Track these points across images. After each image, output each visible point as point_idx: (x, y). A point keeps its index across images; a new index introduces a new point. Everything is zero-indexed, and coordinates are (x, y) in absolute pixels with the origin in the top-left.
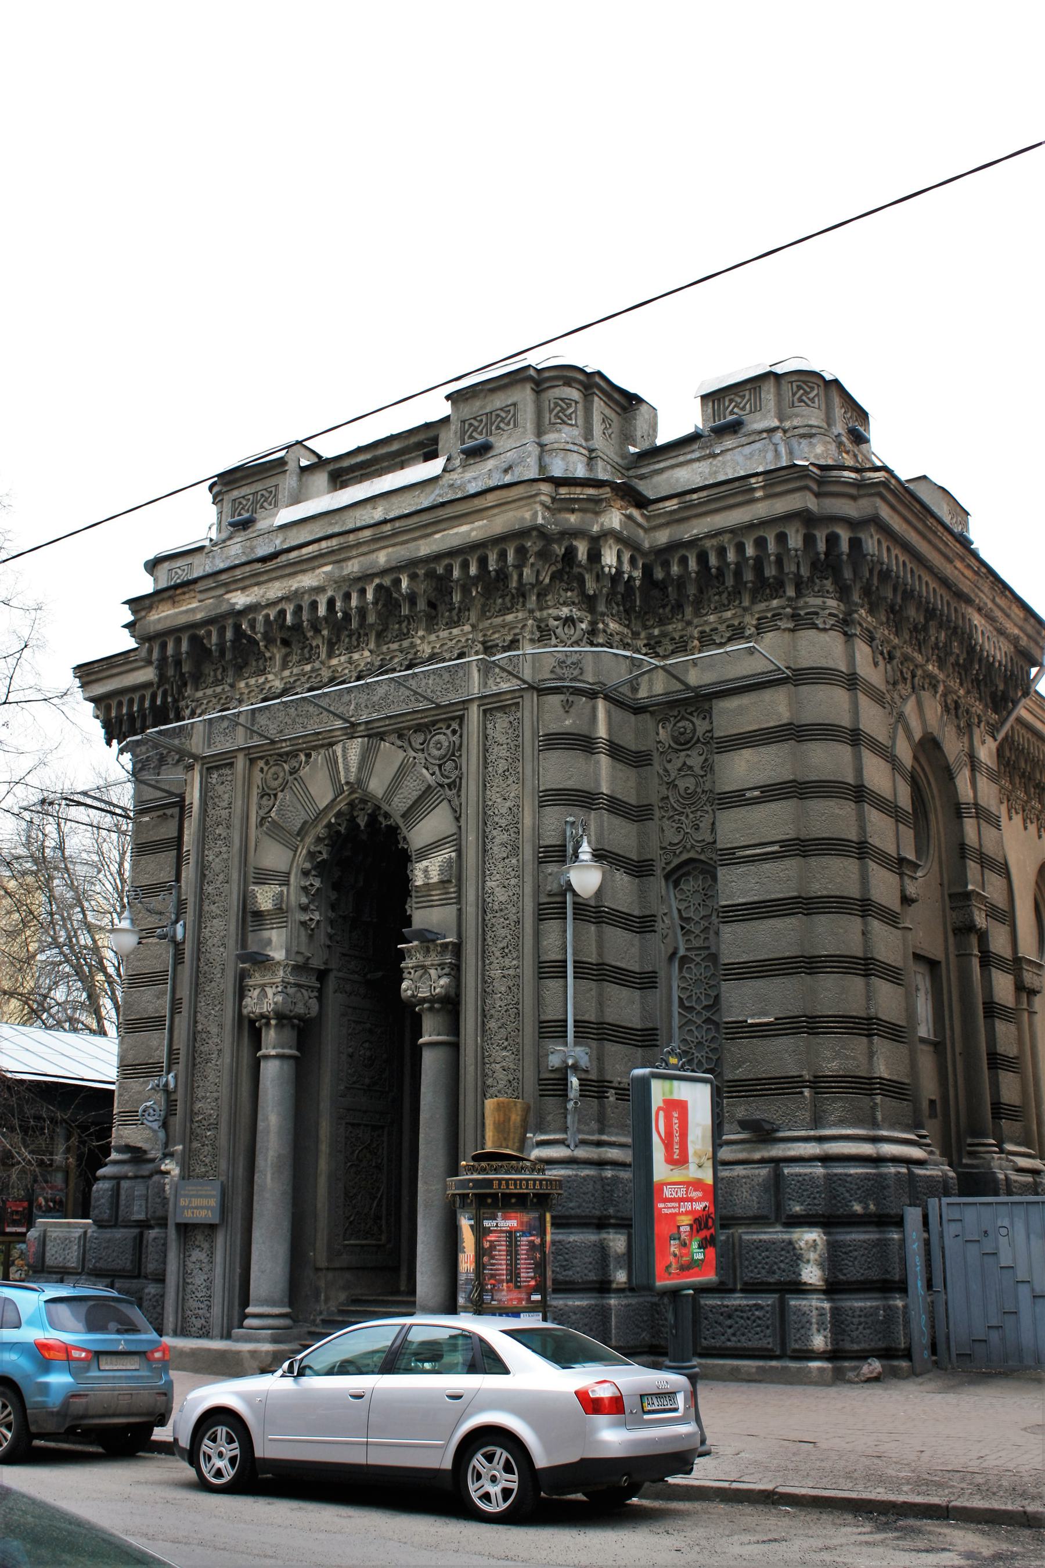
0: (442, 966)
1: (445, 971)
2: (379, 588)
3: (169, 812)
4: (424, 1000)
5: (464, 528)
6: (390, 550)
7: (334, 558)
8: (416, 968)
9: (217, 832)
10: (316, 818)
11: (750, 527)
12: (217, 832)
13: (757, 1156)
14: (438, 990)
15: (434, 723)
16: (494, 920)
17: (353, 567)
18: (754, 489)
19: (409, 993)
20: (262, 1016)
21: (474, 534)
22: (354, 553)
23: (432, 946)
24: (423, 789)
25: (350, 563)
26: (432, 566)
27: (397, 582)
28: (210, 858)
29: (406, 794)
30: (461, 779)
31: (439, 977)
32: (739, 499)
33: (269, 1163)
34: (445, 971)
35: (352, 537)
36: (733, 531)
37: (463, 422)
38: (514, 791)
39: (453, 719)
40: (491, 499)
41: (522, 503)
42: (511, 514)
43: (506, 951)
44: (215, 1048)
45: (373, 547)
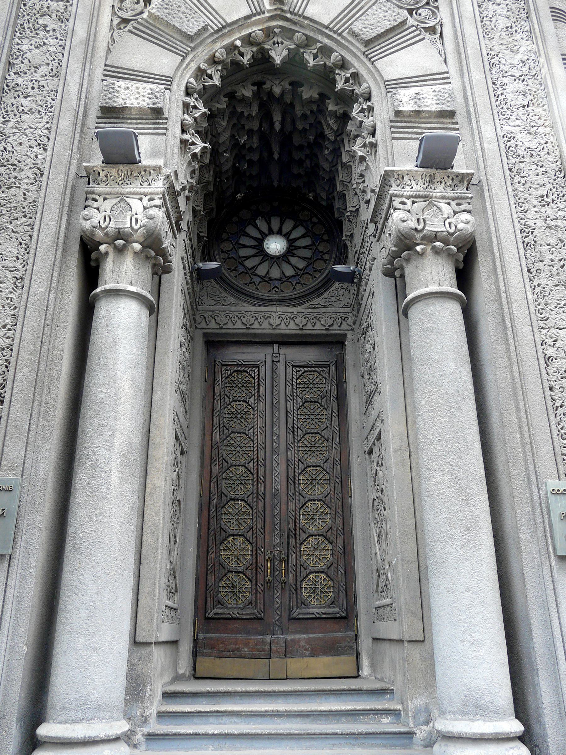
0: (459, 200)
1: (462, 208)
4: (435, 237)
8: (414, 198)
9: (41, 22)
10: (220, 30)
12: (41, 22)
14: (460, 226)
16: (522, 165)
19: (412, 224)
20: (119, 234)
23: (439, 174)
24: (400, 20)
28: (25, 48)
29: (373, 21)
30: (441, 26)
31: (455, 213)
33: (116, 456)
34: (462, 208)
38: (525, 46)
43: (549, 200)
44: (8, 273)
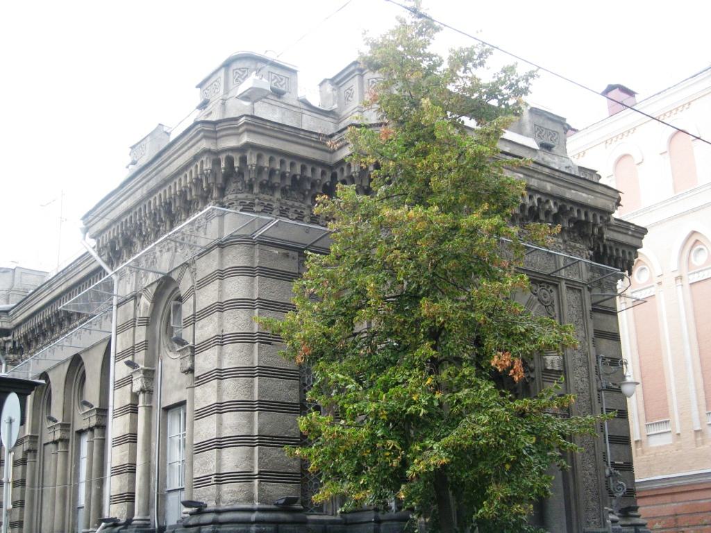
2: (539, 200)
3: (291, 253)
5: (584, 195)
6: (552, 185)
7: (526, 172)
11: (622, 244)
13: (629, 523)
15: (541, 282)
17: (534, 183)
18: (629, 230)
21: (589, 201)
22: (536, 175)
25: (533, 180)
26: (565, 204)
27: (547, 202)
32: (624, 231)
35: (540, 167)
36: (616, 242)
37: (535, 125)
39: (551, 284)
40: (600, 189)
41: (611, 199)
42: (603, 201)
45: (545, 178)
